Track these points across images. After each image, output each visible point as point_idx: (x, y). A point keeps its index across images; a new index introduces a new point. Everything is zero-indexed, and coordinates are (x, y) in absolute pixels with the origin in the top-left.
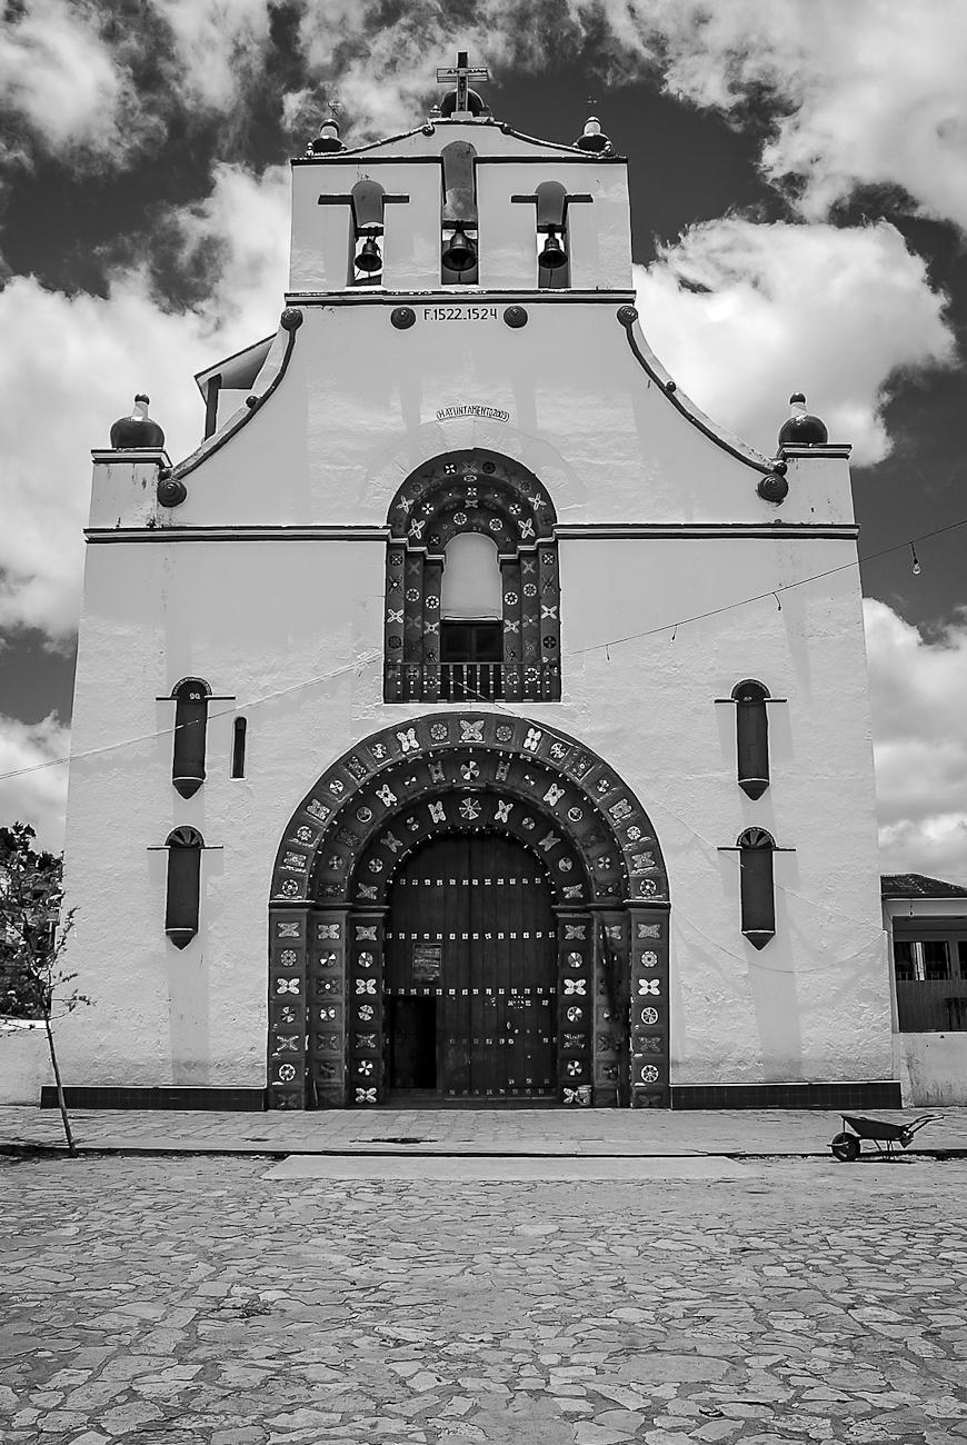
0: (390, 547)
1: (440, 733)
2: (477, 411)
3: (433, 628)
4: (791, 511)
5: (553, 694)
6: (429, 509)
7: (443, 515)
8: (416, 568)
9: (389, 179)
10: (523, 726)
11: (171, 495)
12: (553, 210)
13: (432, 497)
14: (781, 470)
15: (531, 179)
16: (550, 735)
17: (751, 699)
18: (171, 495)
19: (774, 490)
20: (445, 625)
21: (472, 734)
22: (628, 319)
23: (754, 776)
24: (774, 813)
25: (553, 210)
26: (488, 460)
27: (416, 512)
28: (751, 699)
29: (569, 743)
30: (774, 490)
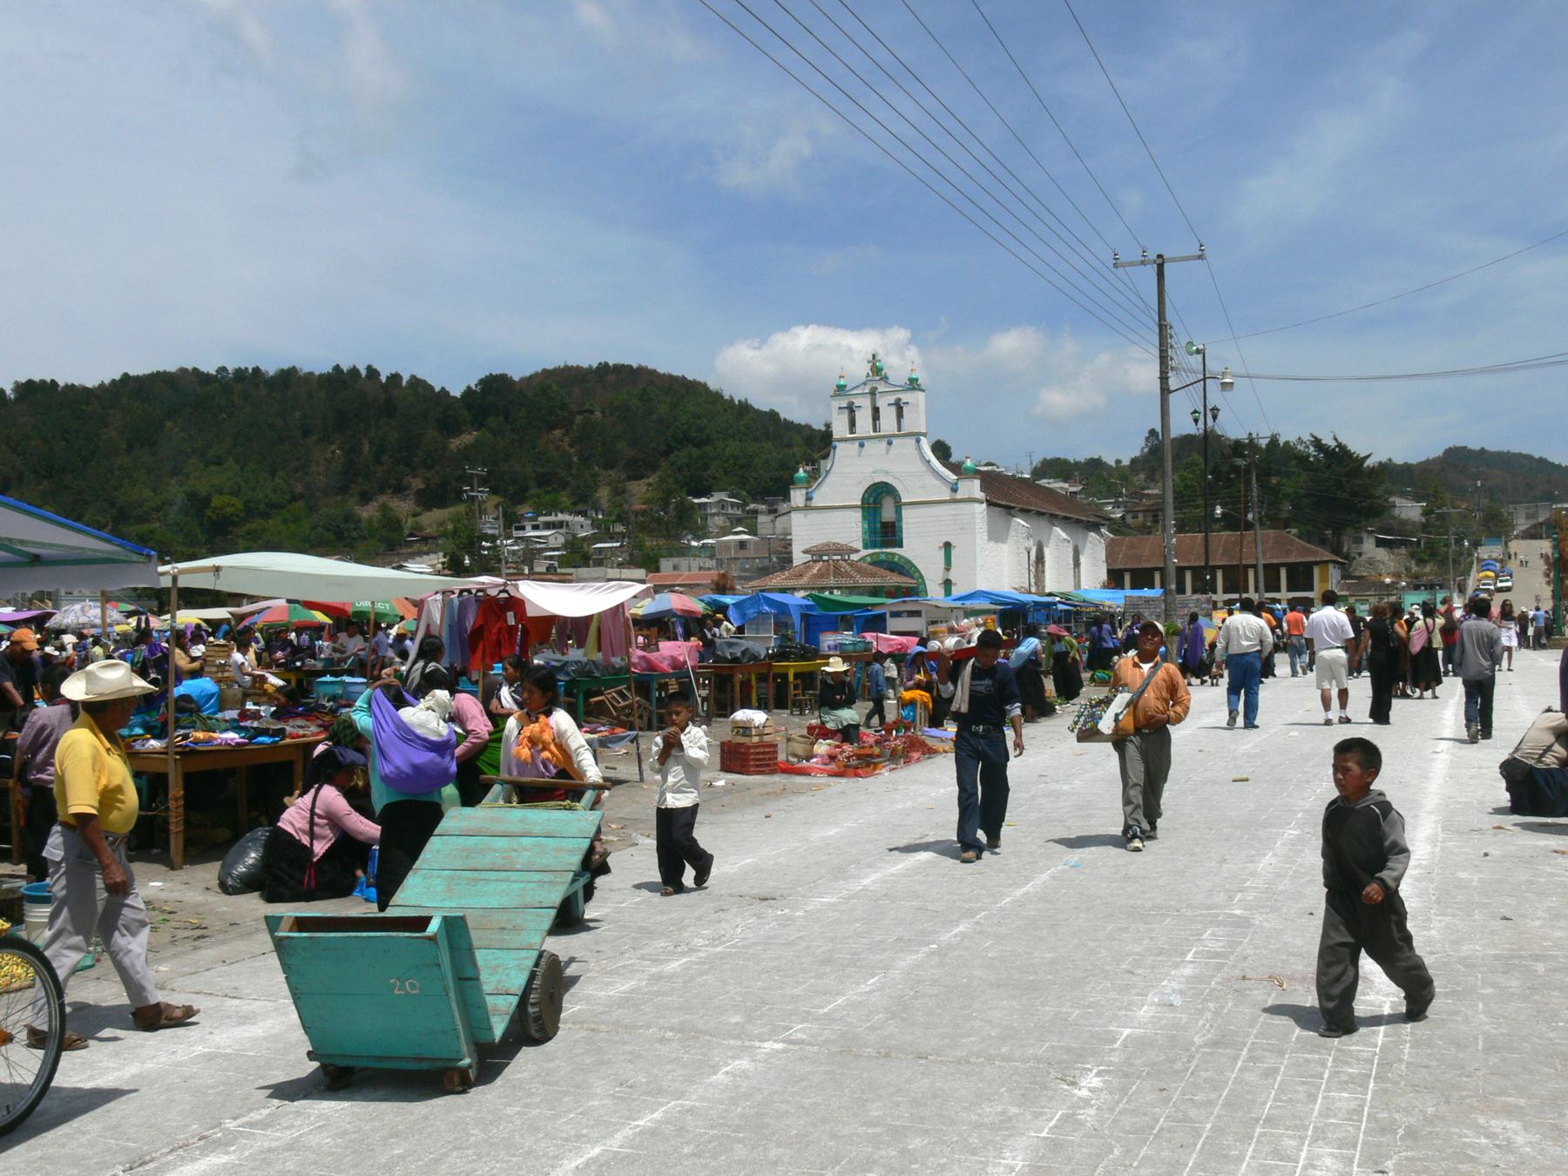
0: (863, 508)
1: (875, 557)
2: (881, 471)
3: (878, 525)
4: (959, 496)
5: (901, 546)
6: (874, 494)
7: (880, 494)
8: (872, 511)
9: (857, 402)
10: (894, 555)
11: (809, 498)
12: (899, 408)
13: (875, 491)
14: (956, 484)
15: (892, 399)
16: (901, 557)
17: (948, 546)
18: (809, 498)
19: (954, 490)
20: (882, 523)
21: (883, 557)
22: (918, 441)
23: (948, 567)
24: (952, 576)
25: (899, 408)
26: (887, 483)
27: (870, 496)
28: (948, 546)
29: (905, 559)
30: (954, 490)
